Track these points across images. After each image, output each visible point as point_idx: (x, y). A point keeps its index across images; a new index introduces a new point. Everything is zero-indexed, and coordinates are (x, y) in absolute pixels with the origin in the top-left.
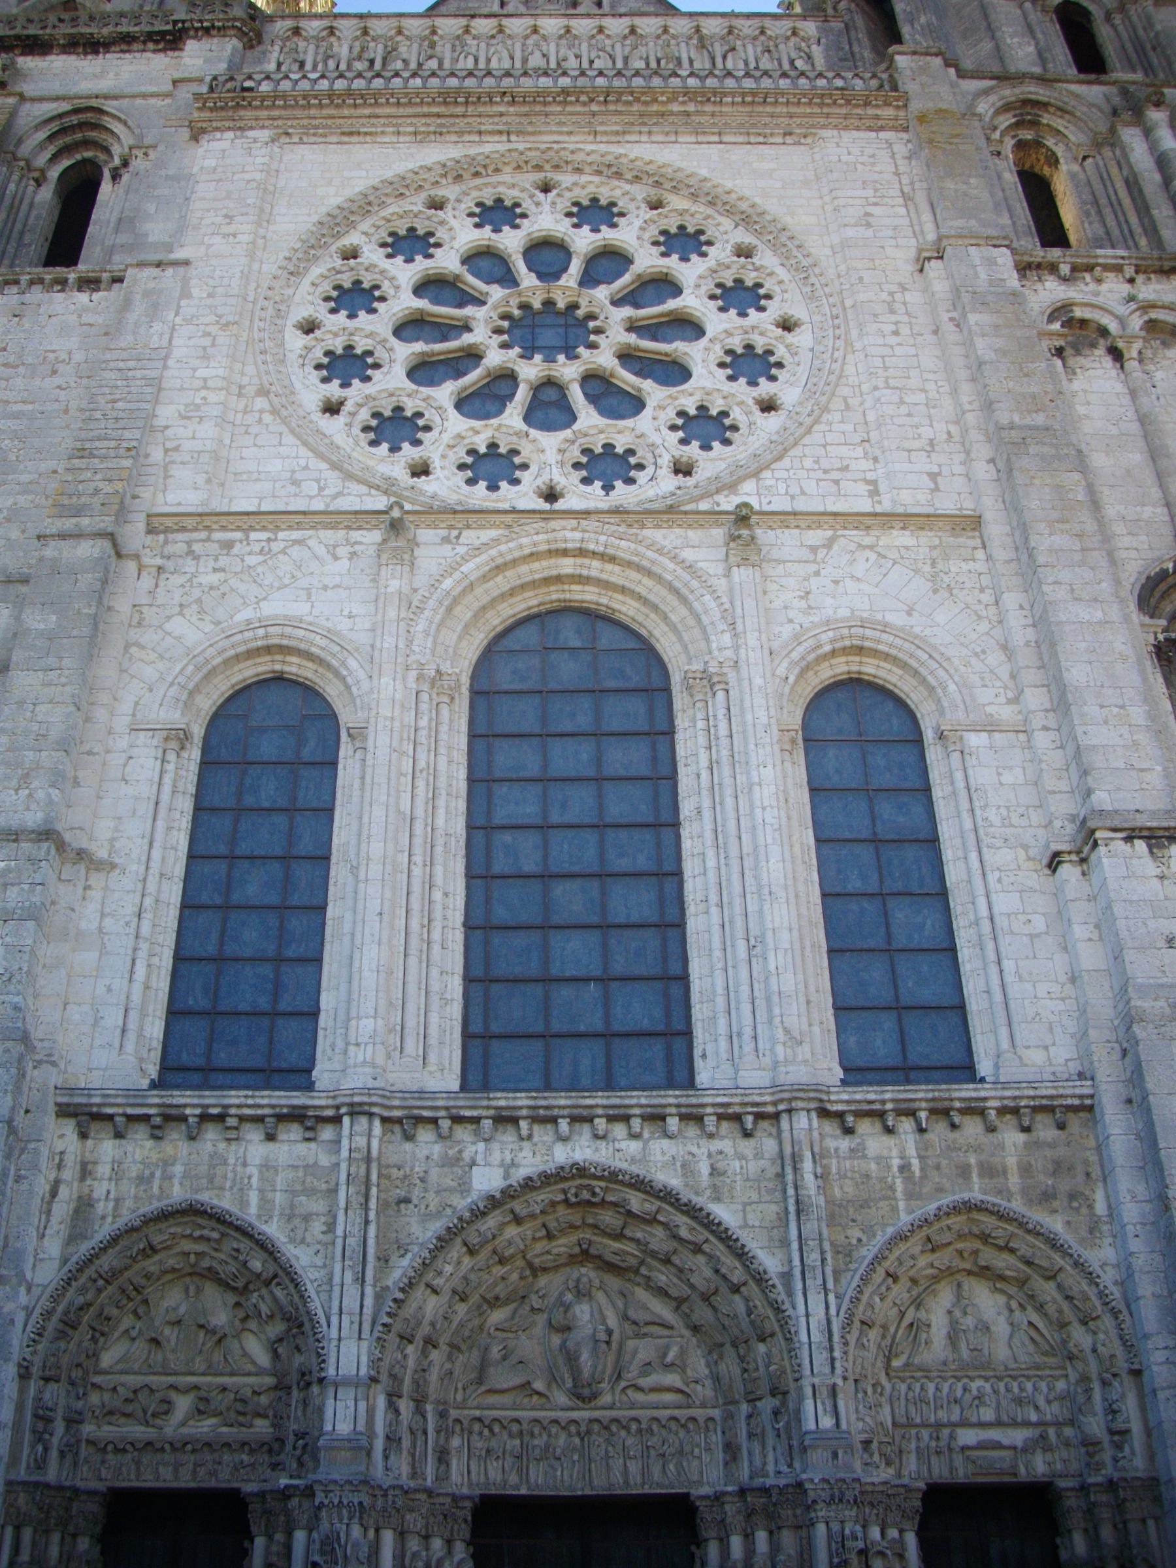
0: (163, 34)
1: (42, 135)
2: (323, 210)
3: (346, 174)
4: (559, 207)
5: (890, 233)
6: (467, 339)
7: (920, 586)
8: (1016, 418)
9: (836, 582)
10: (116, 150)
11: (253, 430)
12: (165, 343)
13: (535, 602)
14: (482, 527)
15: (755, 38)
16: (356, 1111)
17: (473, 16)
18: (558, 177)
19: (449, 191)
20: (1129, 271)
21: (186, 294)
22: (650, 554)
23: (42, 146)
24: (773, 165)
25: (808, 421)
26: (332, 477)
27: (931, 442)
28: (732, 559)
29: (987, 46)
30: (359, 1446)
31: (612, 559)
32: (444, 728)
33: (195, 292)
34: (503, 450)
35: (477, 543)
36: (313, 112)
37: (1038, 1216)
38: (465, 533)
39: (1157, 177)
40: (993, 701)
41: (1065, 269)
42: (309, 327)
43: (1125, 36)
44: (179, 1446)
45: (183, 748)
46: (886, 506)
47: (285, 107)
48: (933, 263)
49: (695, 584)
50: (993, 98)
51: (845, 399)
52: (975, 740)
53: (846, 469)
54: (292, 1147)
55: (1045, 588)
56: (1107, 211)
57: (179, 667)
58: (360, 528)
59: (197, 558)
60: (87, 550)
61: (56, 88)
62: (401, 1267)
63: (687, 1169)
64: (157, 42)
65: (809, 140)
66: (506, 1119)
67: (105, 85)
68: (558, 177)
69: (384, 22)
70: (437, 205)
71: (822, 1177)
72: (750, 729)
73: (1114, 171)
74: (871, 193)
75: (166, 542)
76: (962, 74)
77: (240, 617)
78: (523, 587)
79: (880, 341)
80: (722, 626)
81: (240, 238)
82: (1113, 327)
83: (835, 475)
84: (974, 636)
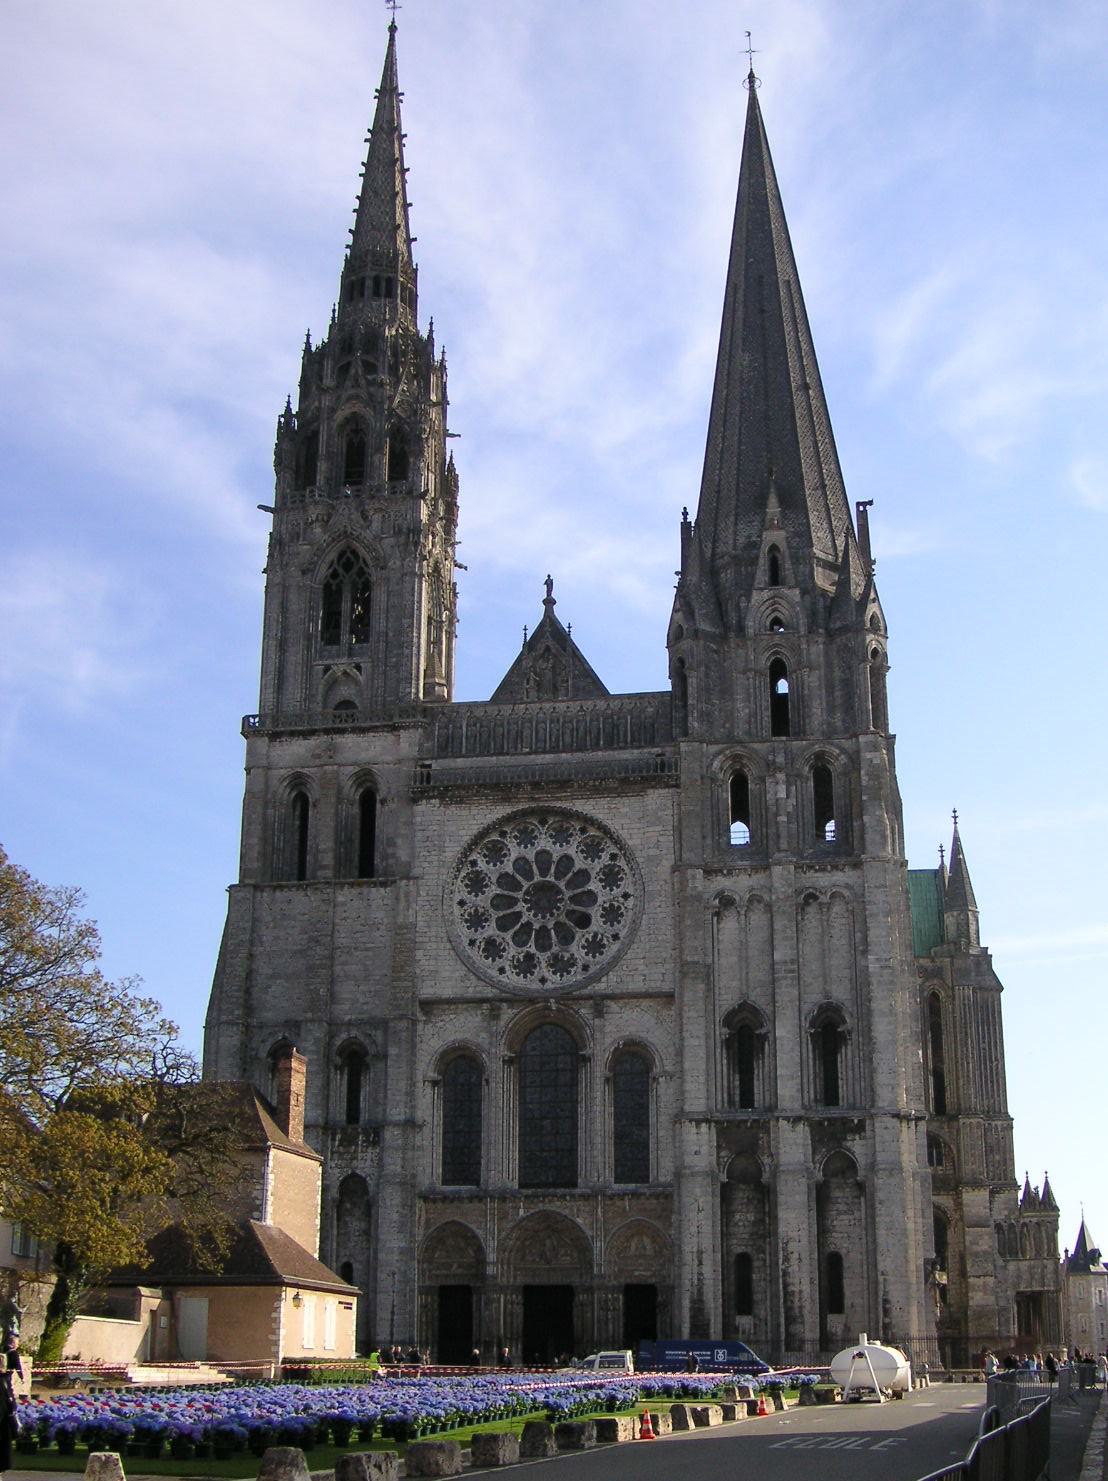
1: (350, 783)
7: (653, 1021)
19: (507, 829)
21: (419, 895)
24: (626, 810)
30: (494, 1277)
39: (775, 809)
42: (462, 903)
44: (455, 1276)
53: (636, 969)
60: (403, 1024)
62: (504, 1234)
76: (710, 743)
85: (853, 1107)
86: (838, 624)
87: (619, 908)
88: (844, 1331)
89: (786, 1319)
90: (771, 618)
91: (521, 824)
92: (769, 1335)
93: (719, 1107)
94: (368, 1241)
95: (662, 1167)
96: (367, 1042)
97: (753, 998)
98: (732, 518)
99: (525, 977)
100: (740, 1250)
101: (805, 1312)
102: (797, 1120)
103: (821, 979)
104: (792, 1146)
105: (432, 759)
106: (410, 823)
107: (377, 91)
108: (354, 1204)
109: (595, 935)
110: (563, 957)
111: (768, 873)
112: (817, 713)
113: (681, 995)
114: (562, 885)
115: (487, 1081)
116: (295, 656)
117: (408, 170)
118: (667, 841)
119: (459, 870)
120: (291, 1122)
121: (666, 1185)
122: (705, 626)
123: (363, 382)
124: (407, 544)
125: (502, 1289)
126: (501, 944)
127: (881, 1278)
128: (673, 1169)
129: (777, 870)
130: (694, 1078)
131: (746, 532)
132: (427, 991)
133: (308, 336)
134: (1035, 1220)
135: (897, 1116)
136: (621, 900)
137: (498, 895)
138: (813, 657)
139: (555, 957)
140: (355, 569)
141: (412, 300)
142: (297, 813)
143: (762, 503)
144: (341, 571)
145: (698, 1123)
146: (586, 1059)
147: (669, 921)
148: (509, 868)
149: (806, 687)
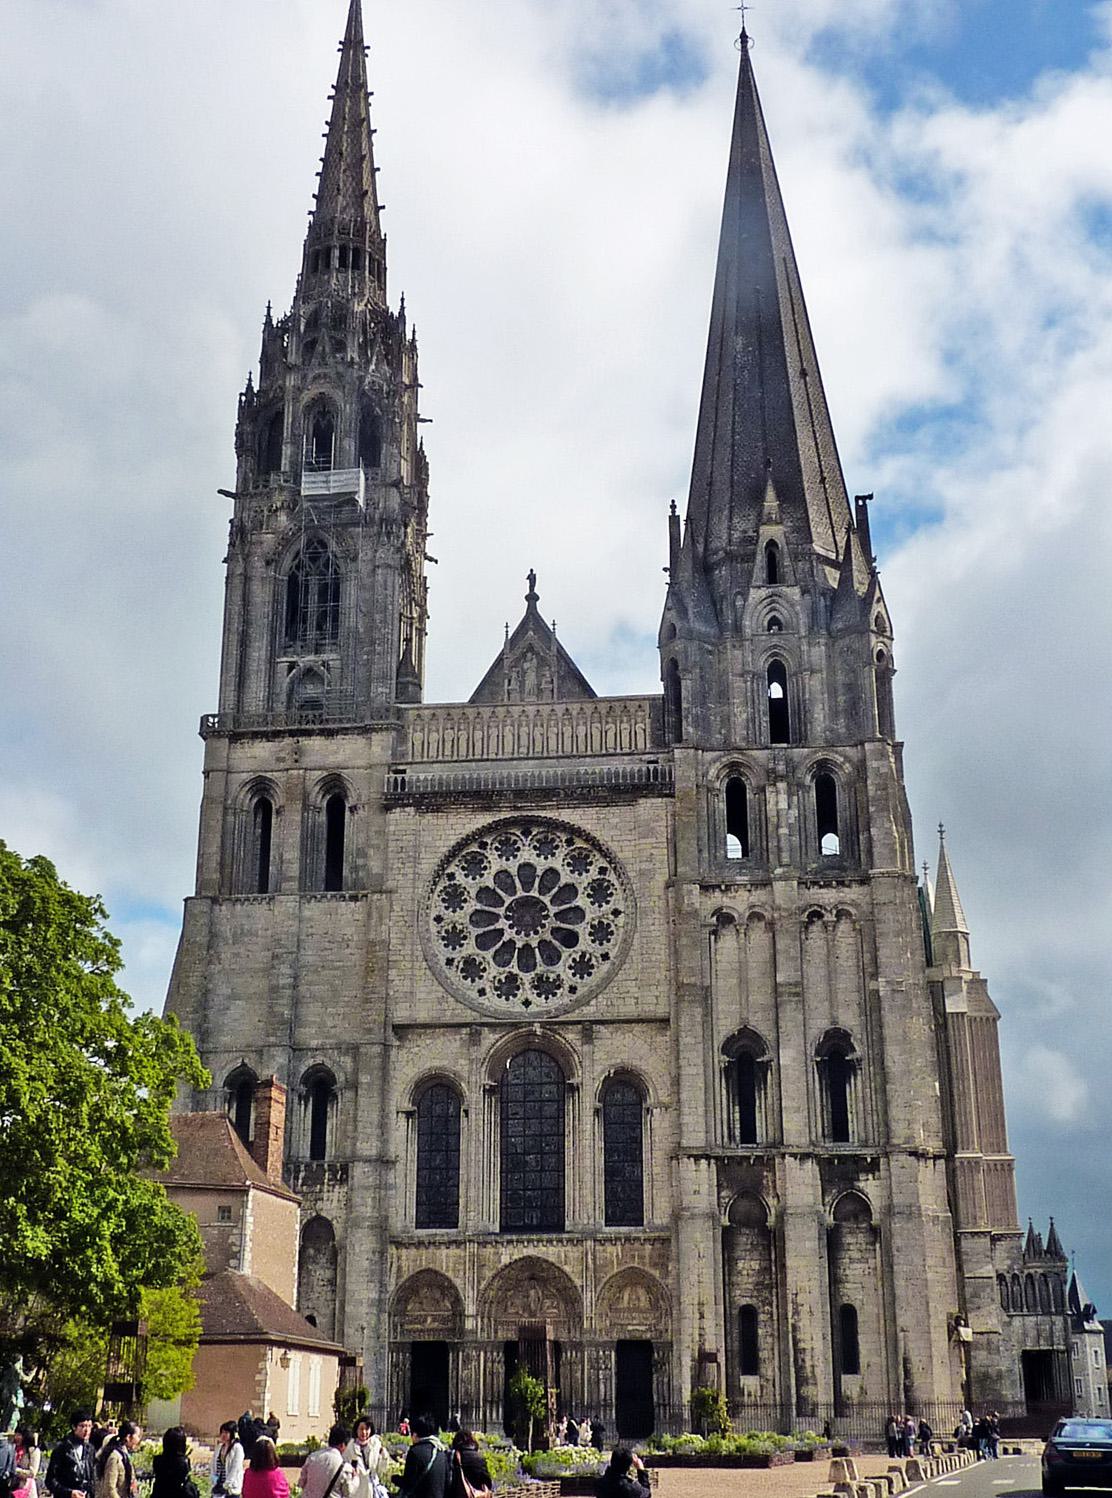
1: (317, 788)
16: (470, 1241)
20: (749, 887)
24: (617, 820)
30: (474, 1332)
37: (652, 1272)
39: (775, 819)
41: (723, 887)
42: (438, 919)
44: (429, 1330)
54: (454, 1251)
62: (484, 1284)
63: (559, 1256)
66: (510, 1242)
71: (594, 1259)
85: (865, 1144)
86: (840, 625)
87: (609, 925)
88: (860, 1396)
89: (797, 1380)
90: (769, 617)
91: (503, 835)
92: (778, 1397)
93: (719, 1142)
94: (334, 1291)
95: (657, 1208)
96: (334, 1069)
97: (754, 1023)
98: (726, 512)
99: (507, 999)
100: (744, 1301)
101: (818, 1371)
102: (804, 1157)
103: (826, 1003)
104: (799, 1187)
105: (407, 764)
106: (382, 833)
107: (340, 43)
108: (318, 1251)
109: (583, 955)
110: (548, 978)
111: (768, 888)
112: (819, 719)
113: (678, 1018)
114: (546, 900)
115: (466, 1112)
116: (259, 652)
117: (375, 131)
118: (662, 853)
119: (435, 884)
120: (270, 1159)
121: (663, 1228)
122: (699, 626)
123: (330, 361)
124: (379, 534)
125: (480, 1346)
126: (481, 963)
127: (901, 1335)
128: (669, 1211)
129: (778, 886)
130: (689, 1112)
131: (742, 525)
132: (401, 1014)
133: (269, 308)
134: (1040, 1271)
135: (914, 1154)
136: (611, 917)
137: (477, 911)
138: (813, 658)
139: (540, 978)
140: (322, 561)
141: (379, 273)
142: (259, 820)
143: (758, 497)
144: (307, 562)
145: (697, 1158)
146: (574, 1089)
147: (663, 940)
148: (488, 880)
149: (807, 690)
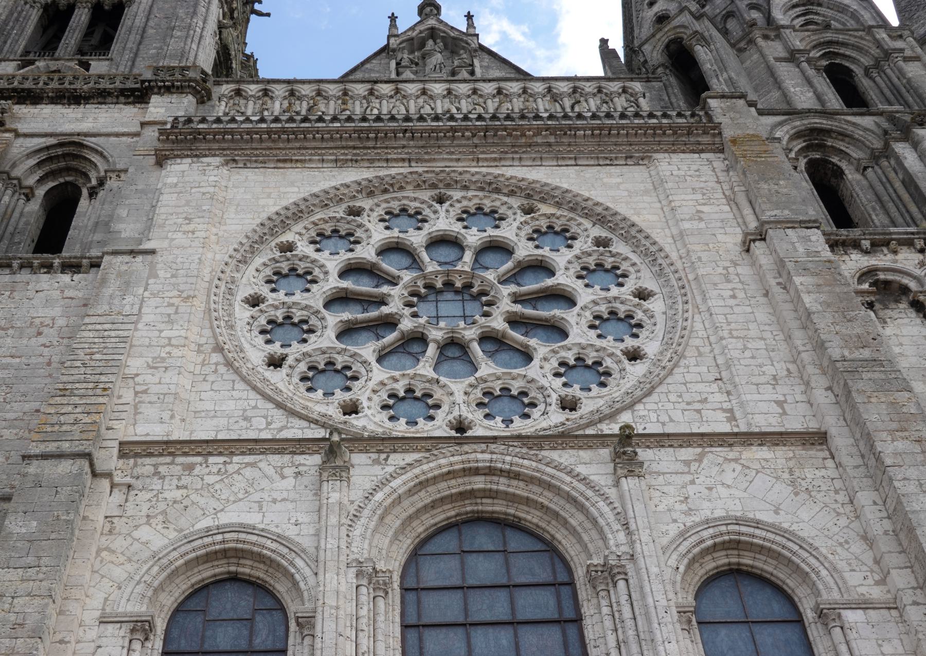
0: (133, 90)
1: (32, 162)
2: (264, 216)
3: (282, 190)
4: (452, 213)
5: (719, 224)
6: (385, 310)
8: (846, 353)
9: (710, 489)
10: (93, 175)
11: (211, 378)
12: (135, 311)
13: (453, 513)
14: (404, 451)
15: (594, 95)
17: (376, 82)
18: (450, 193)
21: (153, 274)
22: (549, 470)
23: (32, 170)
25: (669, 365)
26: (278, 414)
27: (774, 377)
28: (620, 471)
29: (776, 94)
31: (517, 476)
32: (381, 618)
33: (161, 273)
34: (418, 394)
35: (402, 463)
36: (254, 145)
38: (392, 456)
40: (861, 583)
41: (866, 244)
42: (255, 301)
43: (883, 85)
45: (146, 639)
46: (743, 428)
47: (233, 140)
48: (757, 243)
49: (589, 493)
50: (785, 128)
51: (697, 348)
52: (851, 617)
53: (705, 401)
55: (896, 484)
56: (890, 205)
57: (145, 568)
58: (303, 453)
59: (163, 478)
61: (46, 127)
64: (127, 97)
65: (646, 162)
67: (86, 126)
68: (450, 193)
69: (306, 87)
70: (356, 212)
72: (652, 610)
73: (892, 175)
74: (699, 197)
75: (135, 465)
76: (761, 113)
77: (198, 526)
78: (442, 500)
79: (721, 303)
80: (616, 526)
81: (197, 234)
82: (913, 285)
83: (697, 406)
84: (836, 529)
119: (253, 251)
